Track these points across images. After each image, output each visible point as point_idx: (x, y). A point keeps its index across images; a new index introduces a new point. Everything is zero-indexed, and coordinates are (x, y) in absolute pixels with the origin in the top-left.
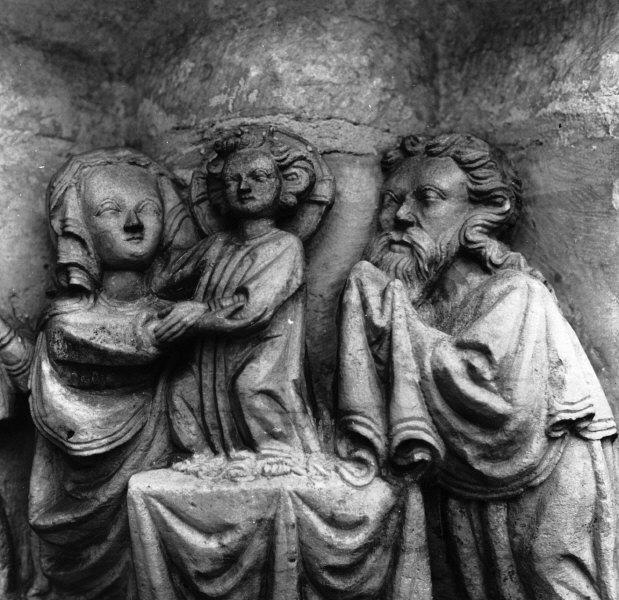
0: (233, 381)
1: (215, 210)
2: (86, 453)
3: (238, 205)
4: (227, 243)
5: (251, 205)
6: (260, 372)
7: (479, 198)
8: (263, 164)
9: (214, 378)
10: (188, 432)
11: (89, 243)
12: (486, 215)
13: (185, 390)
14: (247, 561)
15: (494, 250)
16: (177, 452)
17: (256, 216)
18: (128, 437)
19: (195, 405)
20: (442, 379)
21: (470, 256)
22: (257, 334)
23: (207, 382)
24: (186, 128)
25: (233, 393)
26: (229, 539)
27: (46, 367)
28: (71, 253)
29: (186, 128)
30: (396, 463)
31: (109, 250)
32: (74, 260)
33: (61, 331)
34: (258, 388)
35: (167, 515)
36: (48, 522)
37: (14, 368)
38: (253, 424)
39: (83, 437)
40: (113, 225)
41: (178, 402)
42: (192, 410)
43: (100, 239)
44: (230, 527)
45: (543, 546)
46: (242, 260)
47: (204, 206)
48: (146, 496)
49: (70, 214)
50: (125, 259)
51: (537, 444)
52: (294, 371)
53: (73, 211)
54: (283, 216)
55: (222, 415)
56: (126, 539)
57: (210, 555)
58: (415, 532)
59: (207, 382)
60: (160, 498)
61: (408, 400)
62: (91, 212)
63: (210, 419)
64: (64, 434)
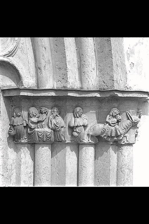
6: (43, 123)
7: (57, 112)
8: (44, 110)
12: (58, 113)
13: (39, 124)
15: (58, 115)
17: (43, 113)
20: (55, 124)
21: (57, 116)
22: (44, 121)
25: (42, 125)
30: (52, 129)
40: (34, 113)
45: (61, 134)
48: (37, 131)
51: (60, 128)
52: (45, 123)
54: (45, 113)
58: (53, 133)
61: (52, 125)
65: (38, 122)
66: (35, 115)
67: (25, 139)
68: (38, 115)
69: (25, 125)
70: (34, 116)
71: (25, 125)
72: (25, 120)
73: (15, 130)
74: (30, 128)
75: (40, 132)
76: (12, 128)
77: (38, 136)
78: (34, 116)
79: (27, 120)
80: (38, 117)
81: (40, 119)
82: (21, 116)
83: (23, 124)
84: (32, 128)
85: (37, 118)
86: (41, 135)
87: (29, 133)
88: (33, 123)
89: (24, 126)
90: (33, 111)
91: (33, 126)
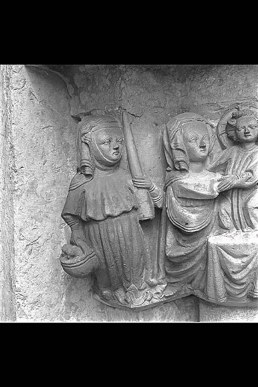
0: (246, 204)
1: (230, 138)
2: (192, 231)
3: (244, 138)
4: (238, 152)
5: (249, 138)
9: (238, 202)
10: (227, 222)
11: (186, 152)
13: (225, 207)
14: (250, 266)
16: (222, 228)
17: (249, 142)
18: (207, 225)
19: (230, 212)
23: (235, 204)
24: (213, 104)
25: (245, 209)
26: (245, 259)
27: (174, 199)
28: (179, 156)
29: (213, 104)
31: (194, 155)
32: (182, 159)
33: (180, 186)
34: (255, 207)
35: (223, 252)
36: (175, 254)
37: (155, 198)
38: (252, 219)
39: (190, 225)
40: (195, 146)
41: (223, 211)
42: (228, 214)
43: (191, 151)
44: (247, 256)
46: (247, 158)
47: (225, 135)
48: (217, 246)
49: (179, 141)
50: (200, 159)
53: (180, 140)
55: (241, 217)
56: (206, 260)
57: (239, 266)
59: (235, 204)
60: (221, 247)
62: (186, 140)
63: (236, 217)
64: (184, 224)
65: (224, 195)
66: (200, 153)
67: (152, 286)
68: (218, 155)
69: (147, 212)
70: (194, 160)
71: (147, 212)
72: (146, 183)
73: (91, 245)
74: (180, 232)
75: (237, 251)
76: (79, 233)
77: (227, 275)
78: (194, 160)
79: (157, 189)
80: (222, 167)
81: (234, 178)
82: (124, 164)
83: (135, 209)
84: (193, 227)
85: (214, 170)
86: (244, 267)
87: (168, 259)
88: (192, 199)
89: (141, 222)
90: (190, 135)
91: (193, 218)
